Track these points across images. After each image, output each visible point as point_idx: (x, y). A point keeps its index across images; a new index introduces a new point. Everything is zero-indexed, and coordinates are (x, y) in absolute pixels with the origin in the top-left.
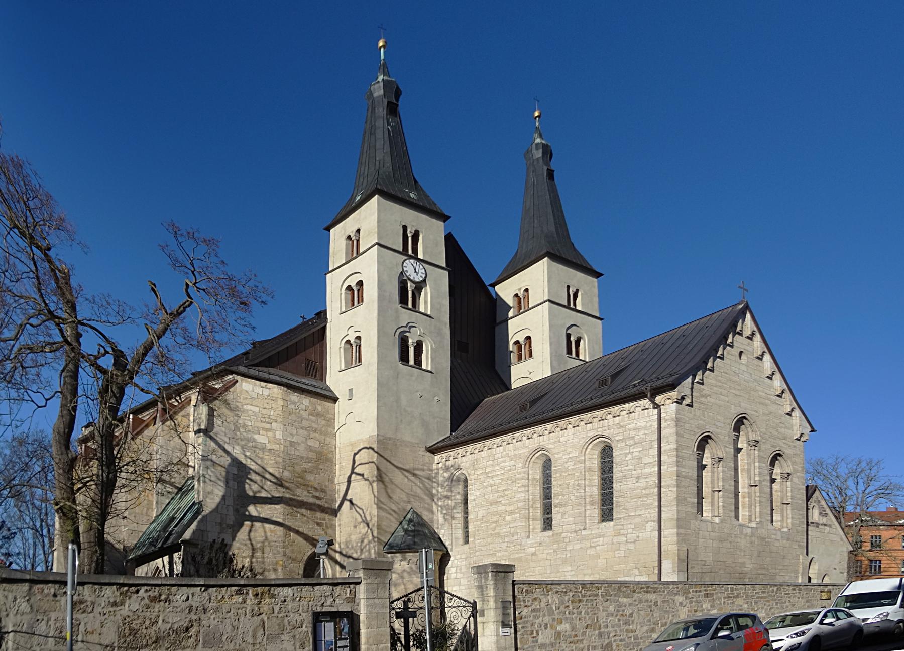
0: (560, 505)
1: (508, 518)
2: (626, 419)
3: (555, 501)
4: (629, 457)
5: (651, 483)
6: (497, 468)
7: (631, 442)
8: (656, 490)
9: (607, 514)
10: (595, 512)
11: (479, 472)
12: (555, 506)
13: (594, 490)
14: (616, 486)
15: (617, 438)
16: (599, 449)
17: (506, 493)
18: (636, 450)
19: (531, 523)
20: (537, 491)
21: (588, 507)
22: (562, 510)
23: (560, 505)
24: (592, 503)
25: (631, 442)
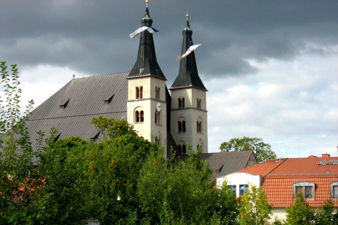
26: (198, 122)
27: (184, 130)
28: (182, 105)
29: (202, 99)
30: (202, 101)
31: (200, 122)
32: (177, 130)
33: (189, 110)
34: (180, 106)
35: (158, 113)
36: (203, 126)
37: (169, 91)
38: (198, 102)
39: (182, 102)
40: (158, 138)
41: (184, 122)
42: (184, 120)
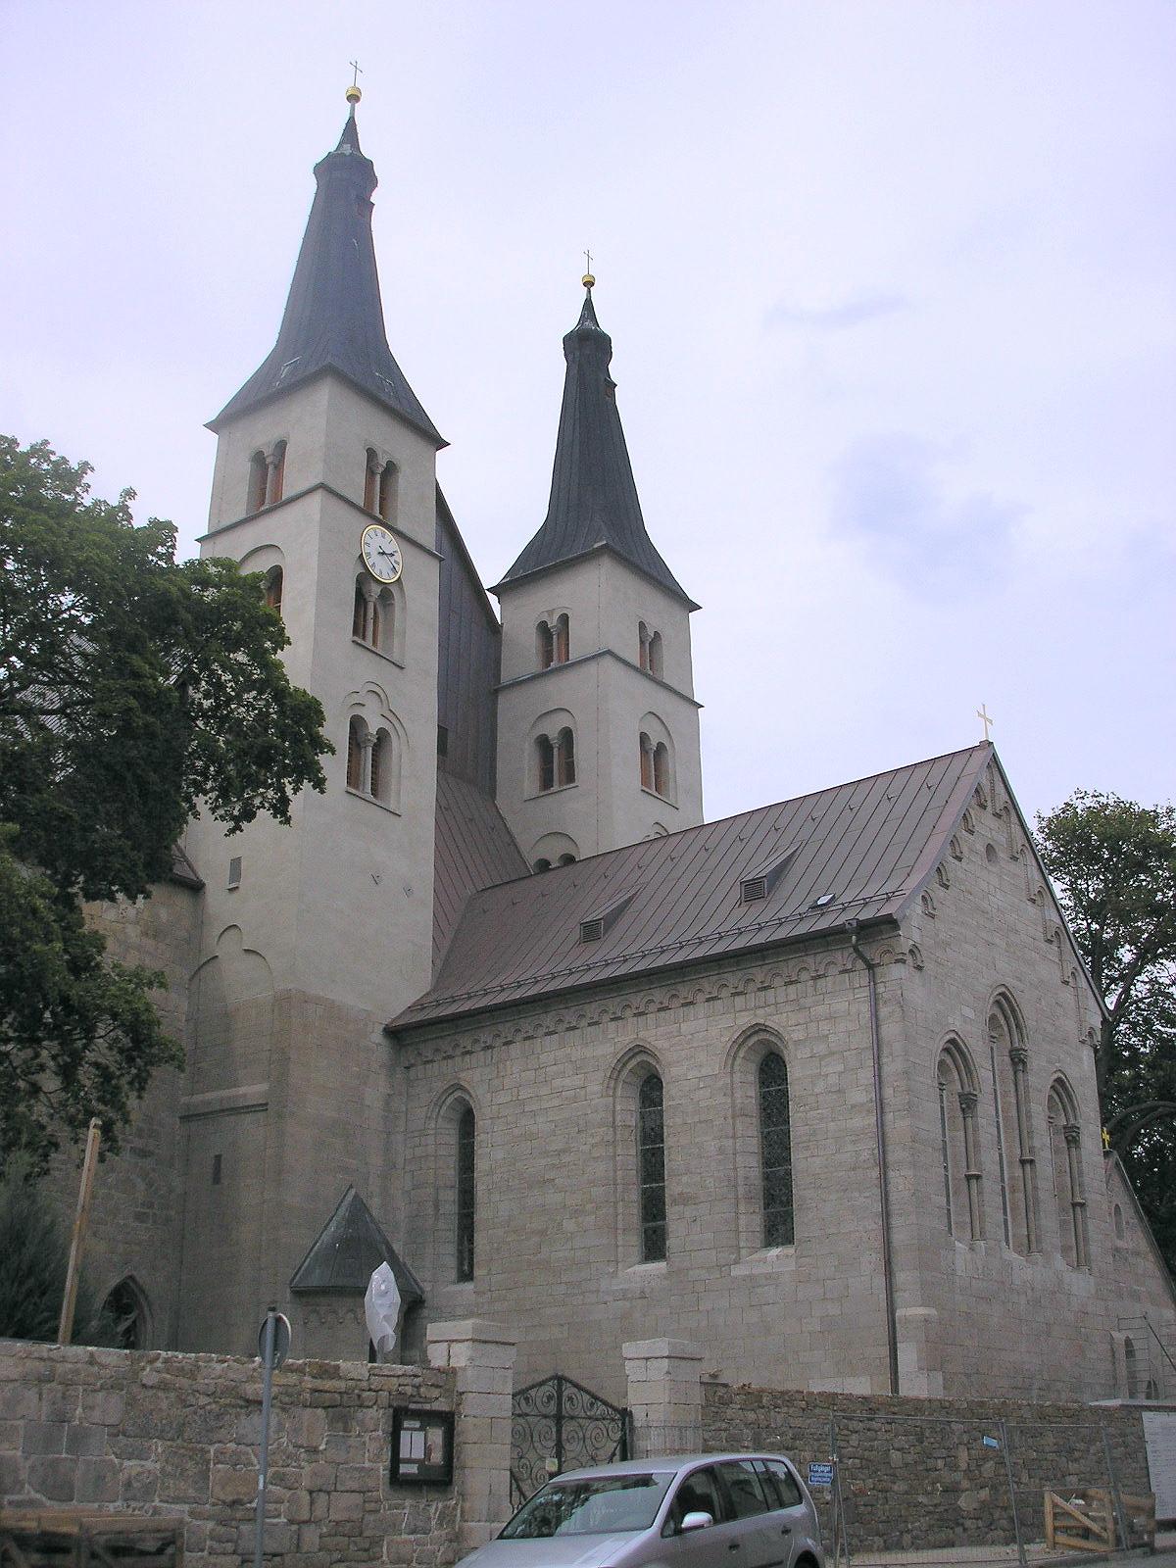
0: (685, 1200)
1: (569, 1225)
2: (810, 990)
3: (673, 1187)
4: (820, 1087)
5: (865, 1155)
6: (544, 1091)
7: (821, 1049)
8: (875, 1173)
9: (778, 1226)
10: (752, 1220)
11: (503, 1098)
12: (675, 1202)
13: (750, 1166)
14: (799, 1159)
15: (795, 1036)
16: (758, 1059)
17: (566, 1158)
18: (834, 1067)
19: (619, 1238)
20: (630, 1155)
21: (742, 1208)
22: (689, 1212)
23: (685, 1200)
24: (749, 1199)
25: (821, 1049)
26: (644, 738)
27: (570, 776)
28: (555, 658)
29: (667, 634)
30: (664, 642)
31: (661, 746)
32: (530, 783)
33: (592, 667)
34: (548, 657)
35: (376, 590)
36: (674, 764)
37: (493, 599)
38: (642, 642)
39: (553, 636)
40: (373, 729)
41: (567, 735)
42: (561, 722)
